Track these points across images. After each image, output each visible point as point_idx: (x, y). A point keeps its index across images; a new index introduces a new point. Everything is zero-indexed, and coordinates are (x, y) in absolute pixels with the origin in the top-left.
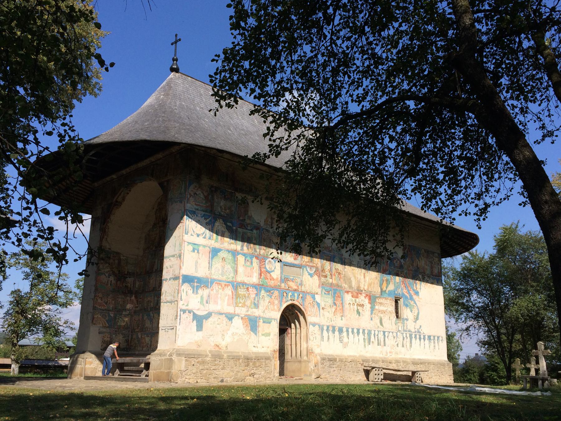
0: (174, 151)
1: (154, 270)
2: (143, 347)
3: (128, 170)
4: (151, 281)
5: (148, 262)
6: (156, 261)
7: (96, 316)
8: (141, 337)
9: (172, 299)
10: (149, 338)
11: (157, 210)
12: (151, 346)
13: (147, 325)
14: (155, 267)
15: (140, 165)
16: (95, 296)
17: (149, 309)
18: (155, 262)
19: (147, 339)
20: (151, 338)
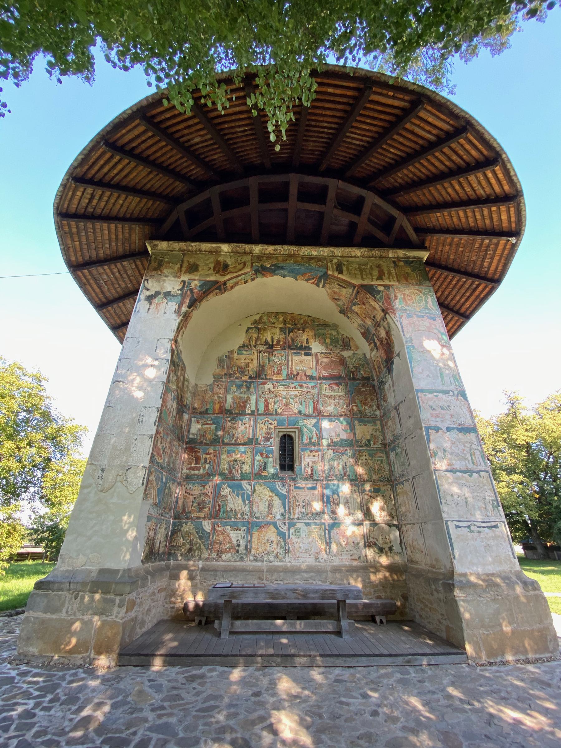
0: (390, 255)
1: (248, 411)
2: (220, 553)
3: (270, 249)
4: (241, 428)
5: (230, 397)
6: (253, 398)
7: (150, 478)
8: (214, 529)
9: (470, 466)
10: (240, 534)
11: (249, 329)
12: (248, 550)
13: (231, 506)
14: (252, 406)
15: (306, 251)
16: (158, 432)
17: (238, 476)
18: (249, 399)
19: (235, 536)
20: (249, 531)
